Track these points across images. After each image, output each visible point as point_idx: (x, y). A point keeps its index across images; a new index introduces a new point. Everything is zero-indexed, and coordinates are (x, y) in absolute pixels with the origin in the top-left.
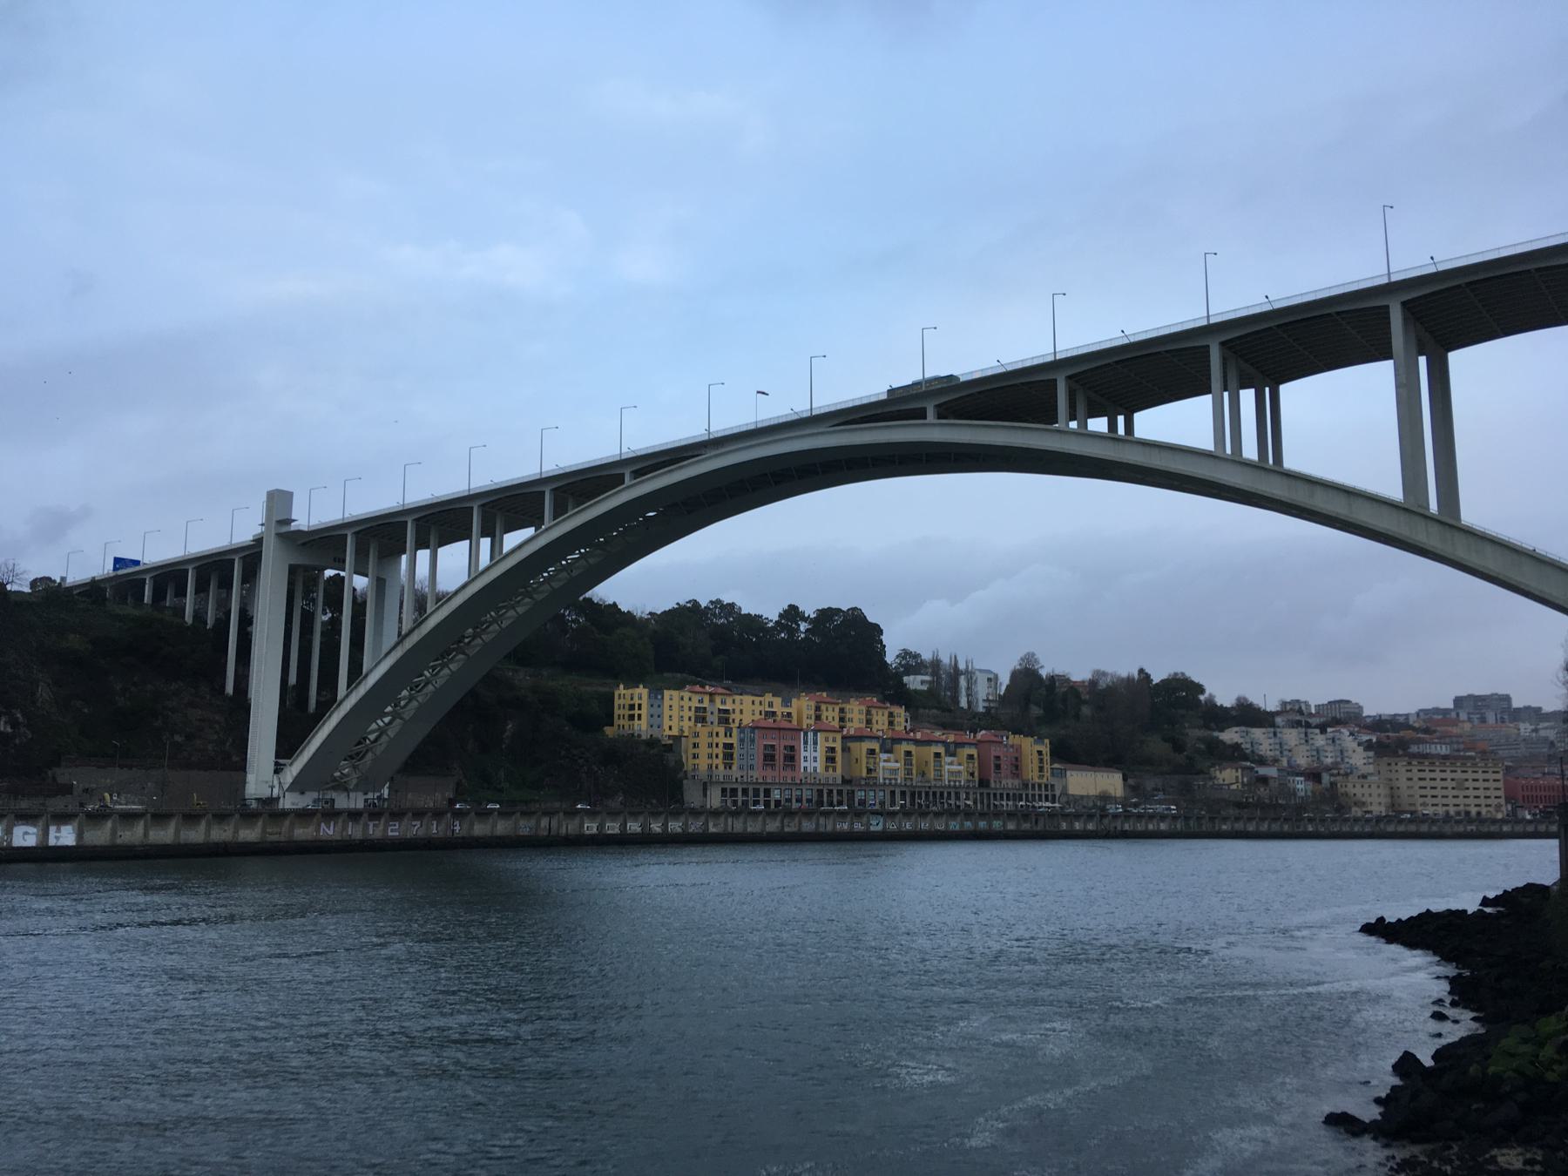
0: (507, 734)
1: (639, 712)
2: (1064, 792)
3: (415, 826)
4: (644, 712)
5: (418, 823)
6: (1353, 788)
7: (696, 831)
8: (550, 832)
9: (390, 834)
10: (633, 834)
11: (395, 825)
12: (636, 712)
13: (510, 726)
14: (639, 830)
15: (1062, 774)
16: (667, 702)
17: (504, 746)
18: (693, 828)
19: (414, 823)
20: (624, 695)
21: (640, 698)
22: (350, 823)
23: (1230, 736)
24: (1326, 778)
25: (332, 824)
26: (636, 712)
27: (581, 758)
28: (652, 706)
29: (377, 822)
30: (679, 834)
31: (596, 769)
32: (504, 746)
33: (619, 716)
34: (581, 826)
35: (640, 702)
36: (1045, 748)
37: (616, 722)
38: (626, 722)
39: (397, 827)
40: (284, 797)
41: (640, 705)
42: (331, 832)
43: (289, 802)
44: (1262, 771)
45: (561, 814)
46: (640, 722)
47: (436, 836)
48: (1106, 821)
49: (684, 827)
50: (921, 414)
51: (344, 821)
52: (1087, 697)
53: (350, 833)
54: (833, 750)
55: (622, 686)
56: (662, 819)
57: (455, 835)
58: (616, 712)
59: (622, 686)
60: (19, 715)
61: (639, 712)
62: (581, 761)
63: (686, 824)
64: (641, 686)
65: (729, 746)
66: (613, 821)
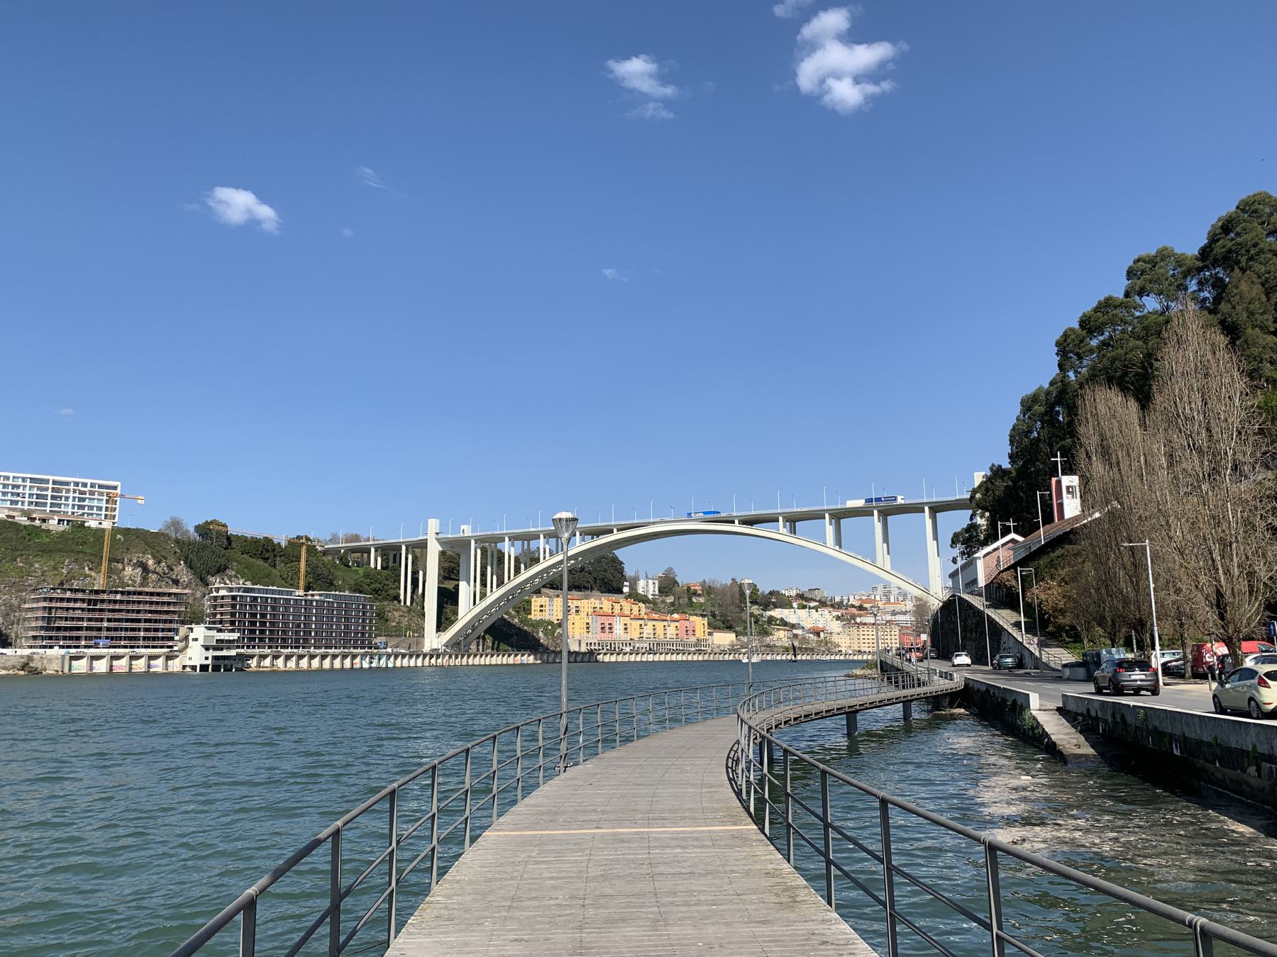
2: (713, 644)
4: (547, 608)
6: (835, 639)
12: (543, 608)
15: (710, 634)
16: (555, 604)
20: (536, 602)
23: (777, 613)
24: (822, 634)
26: (543, 608)
36: (706, 624)
38: (538, 613)
44: (795, 631)
48: (737, 655)
50: (733, 522)
52: (700, 592)
54: (626, 625)
65: (588, 624)
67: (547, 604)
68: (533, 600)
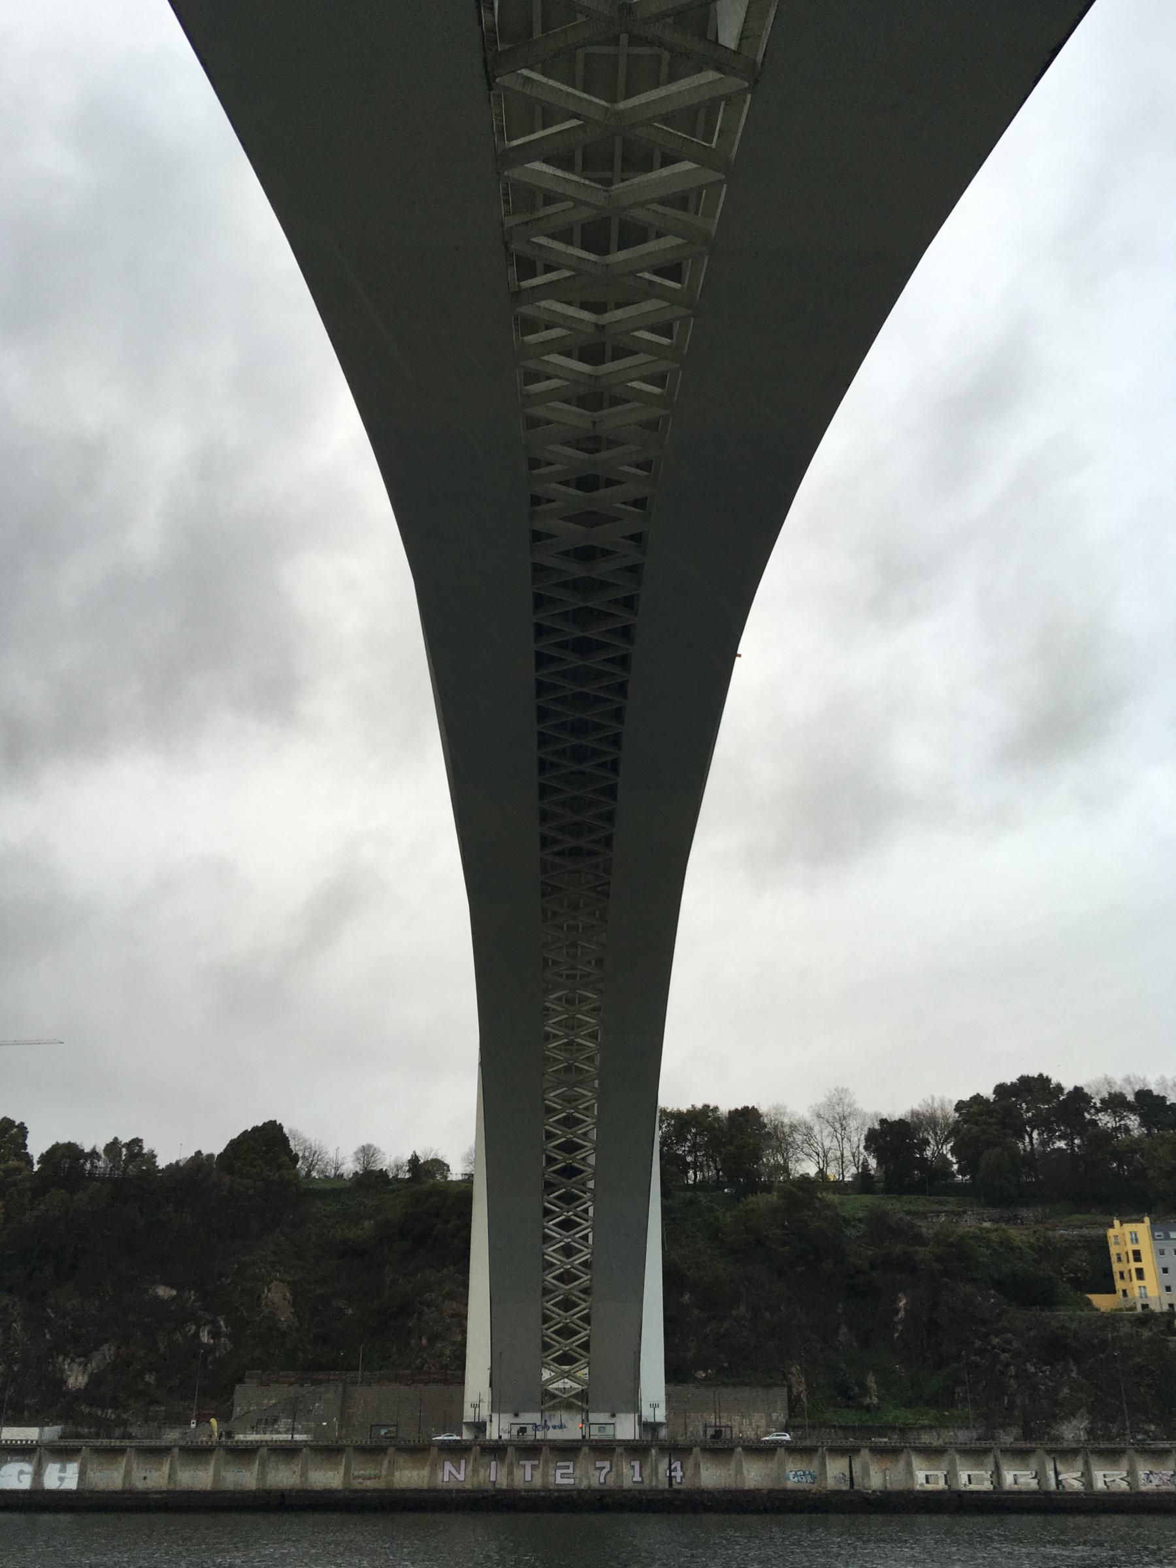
0: (902, 1314)
1: (1138, 1265)
3: (602, 1468)
4: (1148, 1263)
5: (607, 1464)
7: (1164, 1488)
8: (852, 1484)
9: (559, 1481)
10: (1020, 1493)
11: (568, 1467)
13: (904, 1301)
14: (1033, 1485)
17: (896, 1335)
18: (1156, 1482)
19: (599, 1464)
21: (1136, 1240)
22: (493, 1463)
25: (463, 1462)
27: (1003, 1351)
28: (1162, 1253)
29: (536, 1462)
30: (1123, 1494)
31: (1033, 1370)
32: (896, 1335)
33: (1122, 1274)
34: (910, 1473)
35: (1136, 1247)
37: (1119, 1285)
39: (571, 1471)
40: (491, 1421)
41: (1137, 1256)
42: (461, 1477)
43: (499, 1428)
45: (998, 1452)
46: (1141, 1283)
47: (639, 1487)
49: (1129, 1479)
51: (475, 1460)
53: (493, 1478)
55: (1116, 1223)
56: (1079, 1463)
57: (676, 1486)
58: (1116, 1267)
59: (1116, 1223)
60: (222, 1323)
61: (1138, 1265)
62: (1004, 1357)
63: (1132, 1473)
64: (1147, 1219)
66: (980, 1465)
67: (1145, 1245)
68: (1111, 1233)
